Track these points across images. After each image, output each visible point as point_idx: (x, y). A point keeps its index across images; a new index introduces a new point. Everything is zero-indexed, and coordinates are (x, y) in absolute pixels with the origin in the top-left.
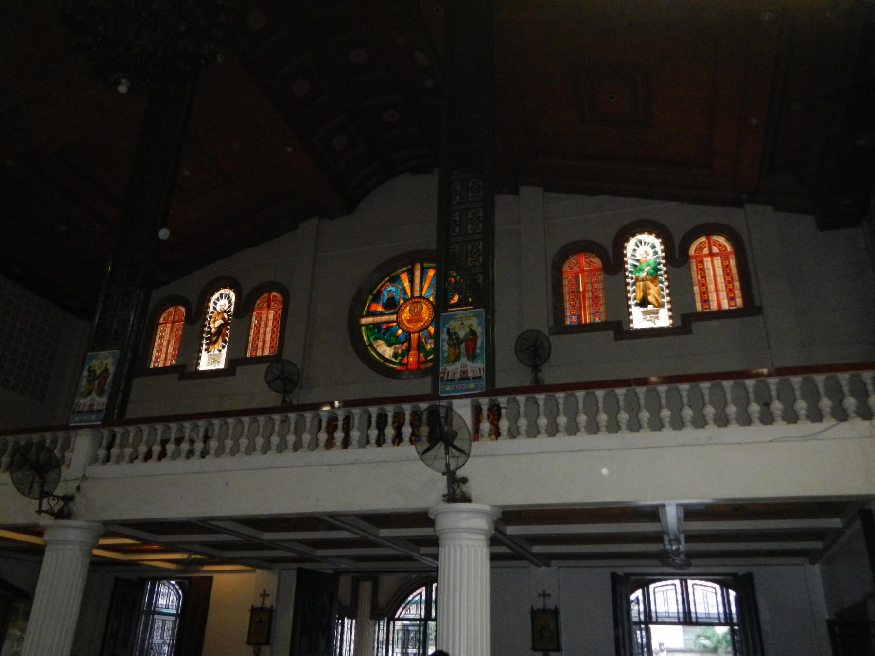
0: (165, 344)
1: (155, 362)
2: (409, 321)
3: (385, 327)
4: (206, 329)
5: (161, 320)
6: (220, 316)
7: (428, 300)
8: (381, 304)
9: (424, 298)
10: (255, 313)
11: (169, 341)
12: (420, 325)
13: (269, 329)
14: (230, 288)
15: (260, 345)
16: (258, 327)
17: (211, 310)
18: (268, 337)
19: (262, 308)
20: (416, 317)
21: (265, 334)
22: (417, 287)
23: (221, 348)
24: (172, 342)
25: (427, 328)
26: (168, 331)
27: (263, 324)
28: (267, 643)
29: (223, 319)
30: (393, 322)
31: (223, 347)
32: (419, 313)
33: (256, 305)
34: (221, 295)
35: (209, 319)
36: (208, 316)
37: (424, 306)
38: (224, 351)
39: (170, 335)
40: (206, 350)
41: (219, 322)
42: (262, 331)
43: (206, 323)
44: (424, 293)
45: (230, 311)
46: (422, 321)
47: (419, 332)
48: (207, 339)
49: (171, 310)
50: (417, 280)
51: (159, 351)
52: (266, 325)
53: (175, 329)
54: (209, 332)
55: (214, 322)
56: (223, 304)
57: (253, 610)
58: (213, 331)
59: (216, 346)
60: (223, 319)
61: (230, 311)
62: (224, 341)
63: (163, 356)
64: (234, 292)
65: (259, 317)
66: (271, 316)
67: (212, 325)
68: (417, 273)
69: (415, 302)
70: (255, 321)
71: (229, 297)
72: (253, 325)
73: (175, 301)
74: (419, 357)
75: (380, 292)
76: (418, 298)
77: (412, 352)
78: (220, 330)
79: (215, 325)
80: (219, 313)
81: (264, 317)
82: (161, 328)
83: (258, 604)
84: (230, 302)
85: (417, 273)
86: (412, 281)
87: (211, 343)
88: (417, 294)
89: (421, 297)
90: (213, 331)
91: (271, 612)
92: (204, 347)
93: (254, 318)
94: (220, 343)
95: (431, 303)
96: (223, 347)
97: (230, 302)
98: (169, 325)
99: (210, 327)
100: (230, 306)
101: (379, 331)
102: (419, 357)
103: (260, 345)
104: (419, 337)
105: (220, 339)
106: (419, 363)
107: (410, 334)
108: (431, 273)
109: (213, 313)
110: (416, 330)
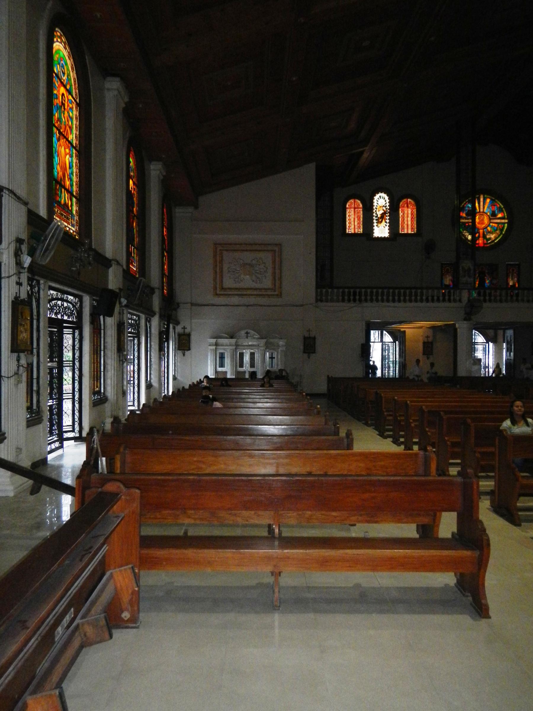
0: (352, 220)
1: (349, 229)
2: (479, 223)
3: (467, 224)
4: (374, 214)
5: (347, 206)
6: (381, 208)
7: (487, 214)
8: (465, 213)
9: (485, 213)
10: (400, 209)
11: (354, 219)
12: (483, 226)
13: (409, 219)
14: (385, 193)
15: (406, 226)
16: (403, 218)
17: (375, 204)
18: (409, 223)
19: (403, 207)
20: (482, 222)
21: (407, 221)
22: (482, 207)
23: (385, 226)
24: (356, 219)
25: (486, 228)
26: (353, 213)
27: (406, 215)
28: (432, 354)
29: (383, 210)
30: (470, 223)
31: (386, 225)
32: (483, 220)
33: (401, 204)
34: (380, 197)
35: (375, 209)
36: (374, 208)
37: (485, 217)
38: (387, 228)
39: (354, 215)
40: (377, 226)
41: (382, 212)
42: (406, 219)
43: (374, 211)
44: (485, 210)
45: (386, 206)
46: (483, 223)
47: (483, 229)
48: (376, 220)
49: (352, 201)
50: (482, 203)
51: (350, 223)
52: (408, 217)
53: (356, 212)
54: (377, 217)
55: (379, 211)
56: (382, 202)
57: (424, 343)
58: (379, 216)
59: (382, 224)
60: (383, 210)
61: (386, 206)
62: (386, 222)
63: (353, 226)
64: (388, 196)
65: (403, 211)
66: (410, 212)
67: (378, 213)
68: (482, 199)
69: (480, 214)
70: (401, 214)
71: (384, 199)
72: (400, 216)
73: (354, 197)
74: (484, 241)
75: (464, 207)
76: (482, 212)
77: (480, 239)
78: (383, 215)
79: (380, 213)
80: (380, 207)
81: (406, 212)
82: (348, 211)
83: (426, 341)
84: (385, 201)
85: (482, 199)
86: (479, 203)
87: (379, 222)
88: (482, 210)
89: (483, 212)
90: (379, 216)
91: (432, 343)
92: (375, 224)
93: (400, 212)
94: (383, 223)
95: (489, 216)
96: (386, 225)
97: (385, 201)
98: (353, 209)
99: (376, 214)
100: (386, 204)
101: (465, 226)
102: (484, 241)
103: (406, 226)
104: (484, 232)
105: (384, 221)
106: (484, 244)
107: (479, 229)
108: (488, 200)
109: (377, 206)
110: (482, 228)
